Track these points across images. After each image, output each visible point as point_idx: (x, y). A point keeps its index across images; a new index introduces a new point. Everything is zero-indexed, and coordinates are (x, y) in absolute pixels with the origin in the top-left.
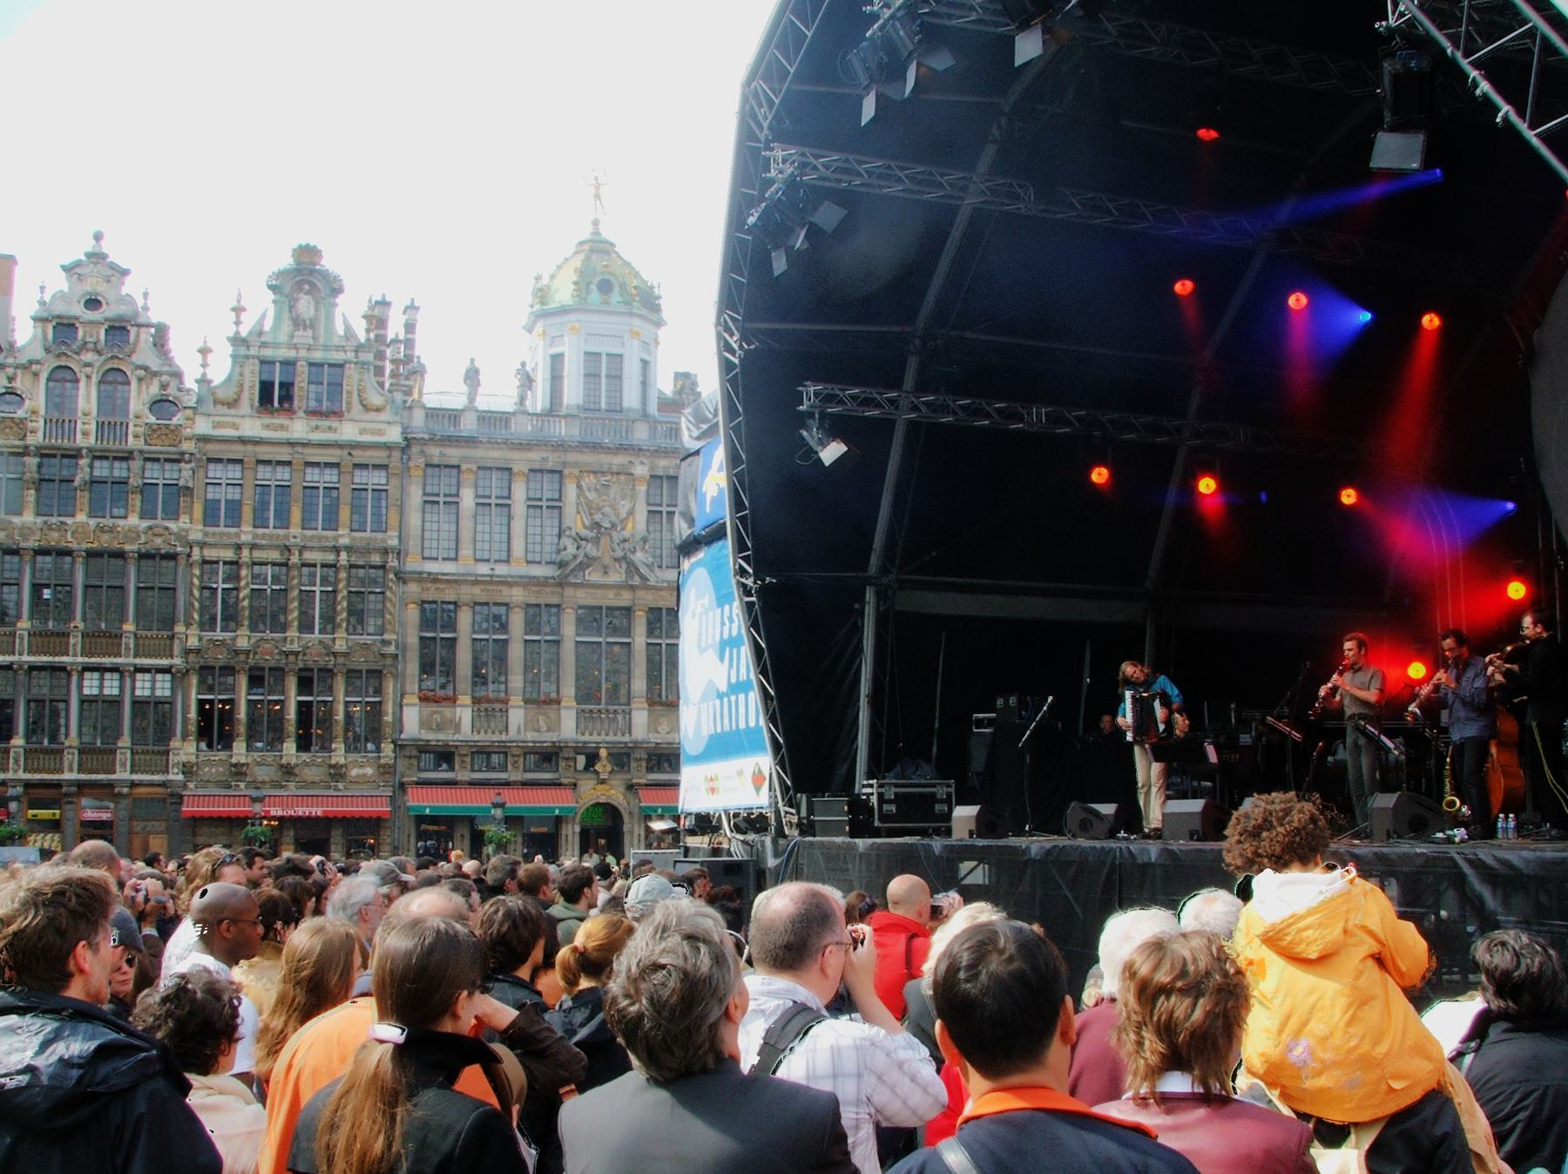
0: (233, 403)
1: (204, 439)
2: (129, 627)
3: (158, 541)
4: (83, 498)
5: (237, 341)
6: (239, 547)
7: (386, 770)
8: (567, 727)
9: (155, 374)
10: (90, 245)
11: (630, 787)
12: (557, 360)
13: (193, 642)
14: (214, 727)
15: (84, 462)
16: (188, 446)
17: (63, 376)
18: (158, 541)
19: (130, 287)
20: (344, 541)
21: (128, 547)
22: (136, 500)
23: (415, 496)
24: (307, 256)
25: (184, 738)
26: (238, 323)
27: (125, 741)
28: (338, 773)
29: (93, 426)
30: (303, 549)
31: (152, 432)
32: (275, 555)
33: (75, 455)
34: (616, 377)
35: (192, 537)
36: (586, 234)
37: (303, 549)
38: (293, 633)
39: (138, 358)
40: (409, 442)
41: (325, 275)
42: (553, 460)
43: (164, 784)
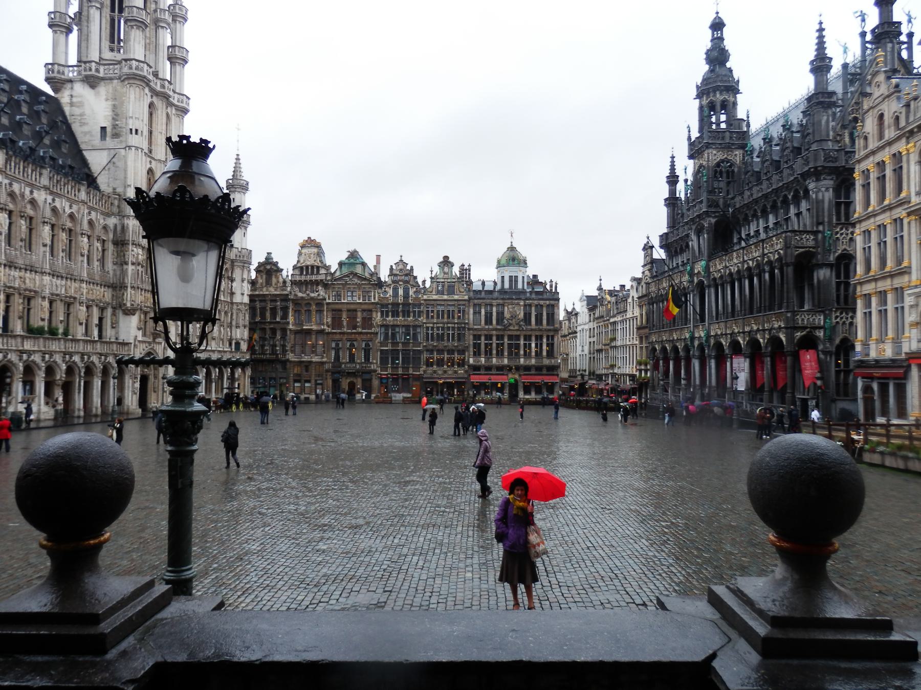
1: (425, 300)
4: (401, 314)
5: (432, 278)
7: (466, 372)
8: (506, 361)
11: (520, 375)
12: (503, 277)
14: (429, 364)
23: (471, 311)
24: (446, 258)
28: (456, 372)
33: (398, 304)
34: (516, 281)
36: (509, 245)
40: (470, 299)
41: (450, 262)
42: (501, 302)
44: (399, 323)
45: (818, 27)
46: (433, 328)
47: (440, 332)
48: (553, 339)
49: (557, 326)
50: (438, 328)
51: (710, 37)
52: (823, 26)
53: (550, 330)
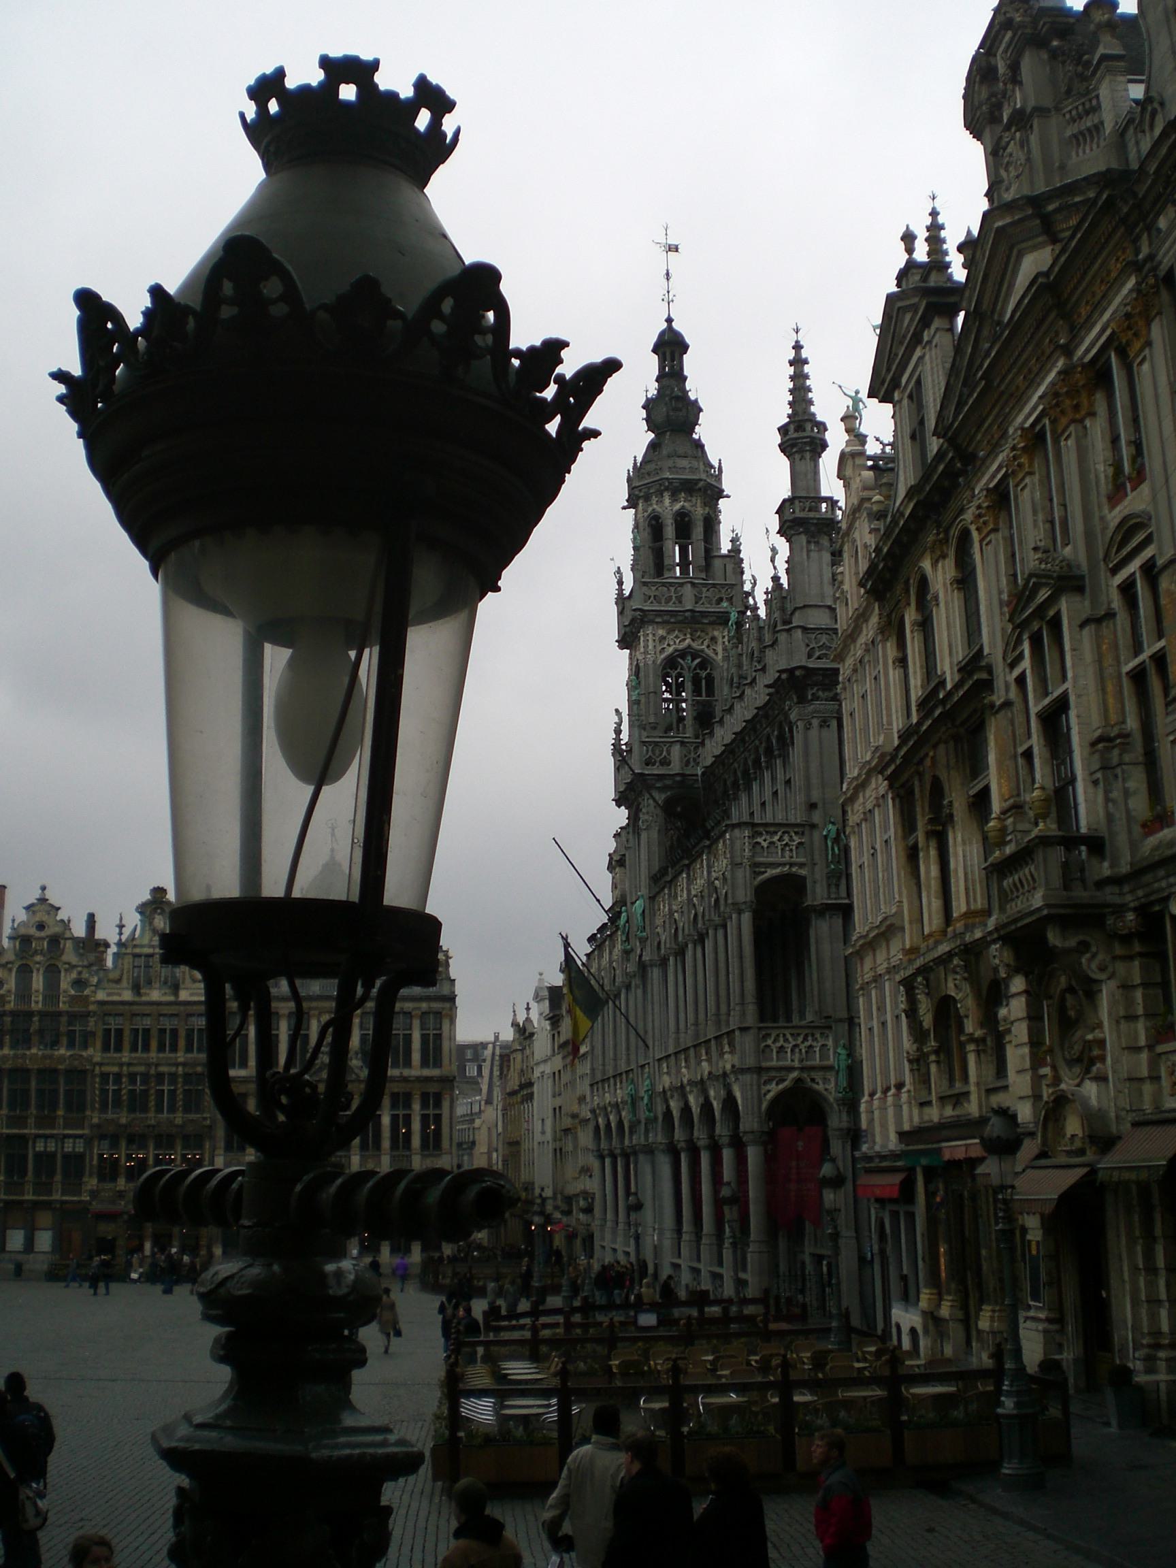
0: (118, 981)
1: (102, 1003)
2: (60, 1113)
3: (76, 1063)
4: (35, 1039)
6: (121, 1065)
9: (75, 966)
10: (37, 894)
13: (95, 1121)
15: (36, 1019)
16: (92, 1008)
17: (25, 972)
18: (76, 1063)
19: (62, 915)
20: (181, 1060)
21: (60, 1067)
22: (64, 1040)
25: (91, 1175)
26: (121, 934)
27: (58, 1177)
29: (41, 998)
30: (157, 1065)
31: (73, 1000)
32: (142, 1069)
33: (30, 1014)
35: (97, 1059)
37: (157, 1065)
38: (151, 1114)
39: (65, 958)
43: (79, 1202)
44: (29, 1064)
45: (791, 354)
46: (118, 1076)
47: (139, 1087)
48: (438, 1104)
49: (449, 1067)
50: (132, 1077)
51: (655, 372)
52: (804, 354)
53: (428, 1079)
